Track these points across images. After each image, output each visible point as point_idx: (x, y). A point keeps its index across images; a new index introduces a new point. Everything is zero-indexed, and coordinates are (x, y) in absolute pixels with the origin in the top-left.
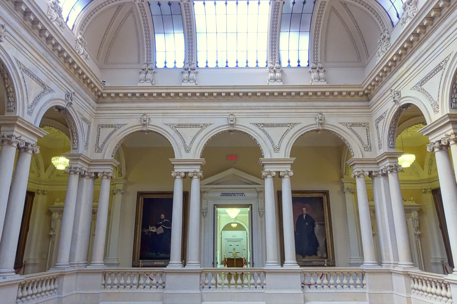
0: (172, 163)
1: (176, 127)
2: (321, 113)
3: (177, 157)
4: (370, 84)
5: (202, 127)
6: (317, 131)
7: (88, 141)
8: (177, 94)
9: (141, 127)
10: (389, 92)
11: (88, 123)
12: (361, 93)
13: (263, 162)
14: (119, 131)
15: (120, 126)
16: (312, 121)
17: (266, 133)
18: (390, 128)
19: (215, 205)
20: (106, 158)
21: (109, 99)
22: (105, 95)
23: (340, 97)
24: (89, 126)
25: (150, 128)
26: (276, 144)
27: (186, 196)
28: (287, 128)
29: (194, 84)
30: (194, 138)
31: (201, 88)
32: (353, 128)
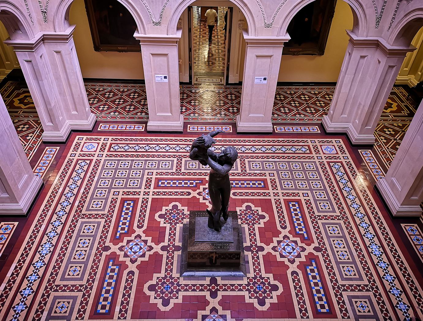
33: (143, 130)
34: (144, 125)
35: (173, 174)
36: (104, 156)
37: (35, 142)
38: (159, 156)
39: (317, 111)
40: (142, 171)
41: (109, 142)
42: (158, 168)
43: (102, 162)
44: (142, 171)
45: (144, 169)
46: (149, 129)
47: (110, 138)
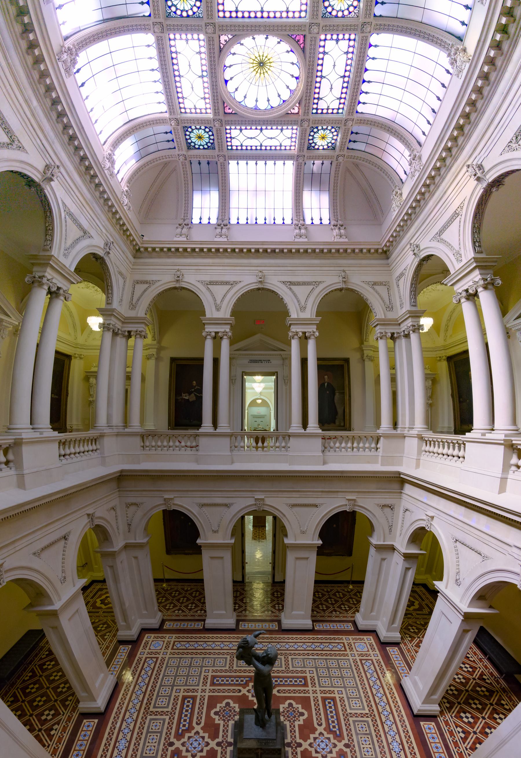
0: (203, 322)
1: (207, 284)
2: (344, 271)
3: (208, 315)
4: (389, 241)
5: (232, 284)
6: (341, 290)
7: (122, 297)
8: (209, 250)
9: (175, 283)
10: (409, 246)
11: (124, 278)
12: (380, 251)
13: (290, 322)
14: (153, 287)
15: (154, 282)
16: (336, 279)
17: (293, 292)
18: (412, 284)
19: (243, 372)
20: (139, 316)
21: (146, 254)
22: (142, 249)
23: (360, 255)
24: (124, 281)
25: (184, 285)
26: (303, 303)
27: (216, 362)
28: (312, 287)
29: (226, 240)
30: (225, 296)
31: (233, 243)
32: (375, 287)
33: (202, 628)
34: (203, 623)
35: (226, 671)
36: (168, 653)
37: (111, 641)
38: (215, 654)
39: (350, 608)
40: (200, 668)
41: (173, 640)
42: (214, 666)
43: (166, 659)
44: (200, 668)
45: (202, 667)
46: (207, 626)
47: (174, 636)
